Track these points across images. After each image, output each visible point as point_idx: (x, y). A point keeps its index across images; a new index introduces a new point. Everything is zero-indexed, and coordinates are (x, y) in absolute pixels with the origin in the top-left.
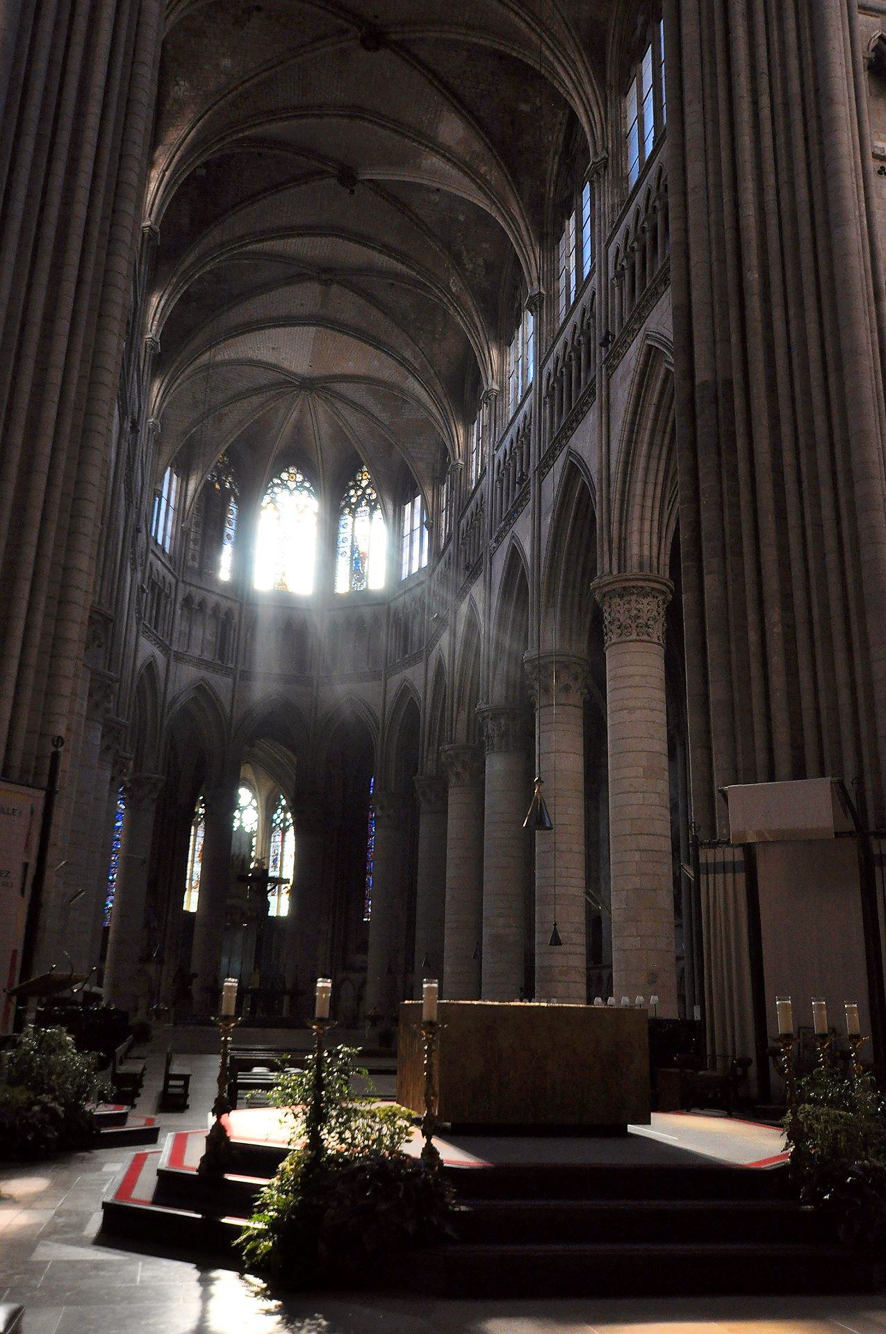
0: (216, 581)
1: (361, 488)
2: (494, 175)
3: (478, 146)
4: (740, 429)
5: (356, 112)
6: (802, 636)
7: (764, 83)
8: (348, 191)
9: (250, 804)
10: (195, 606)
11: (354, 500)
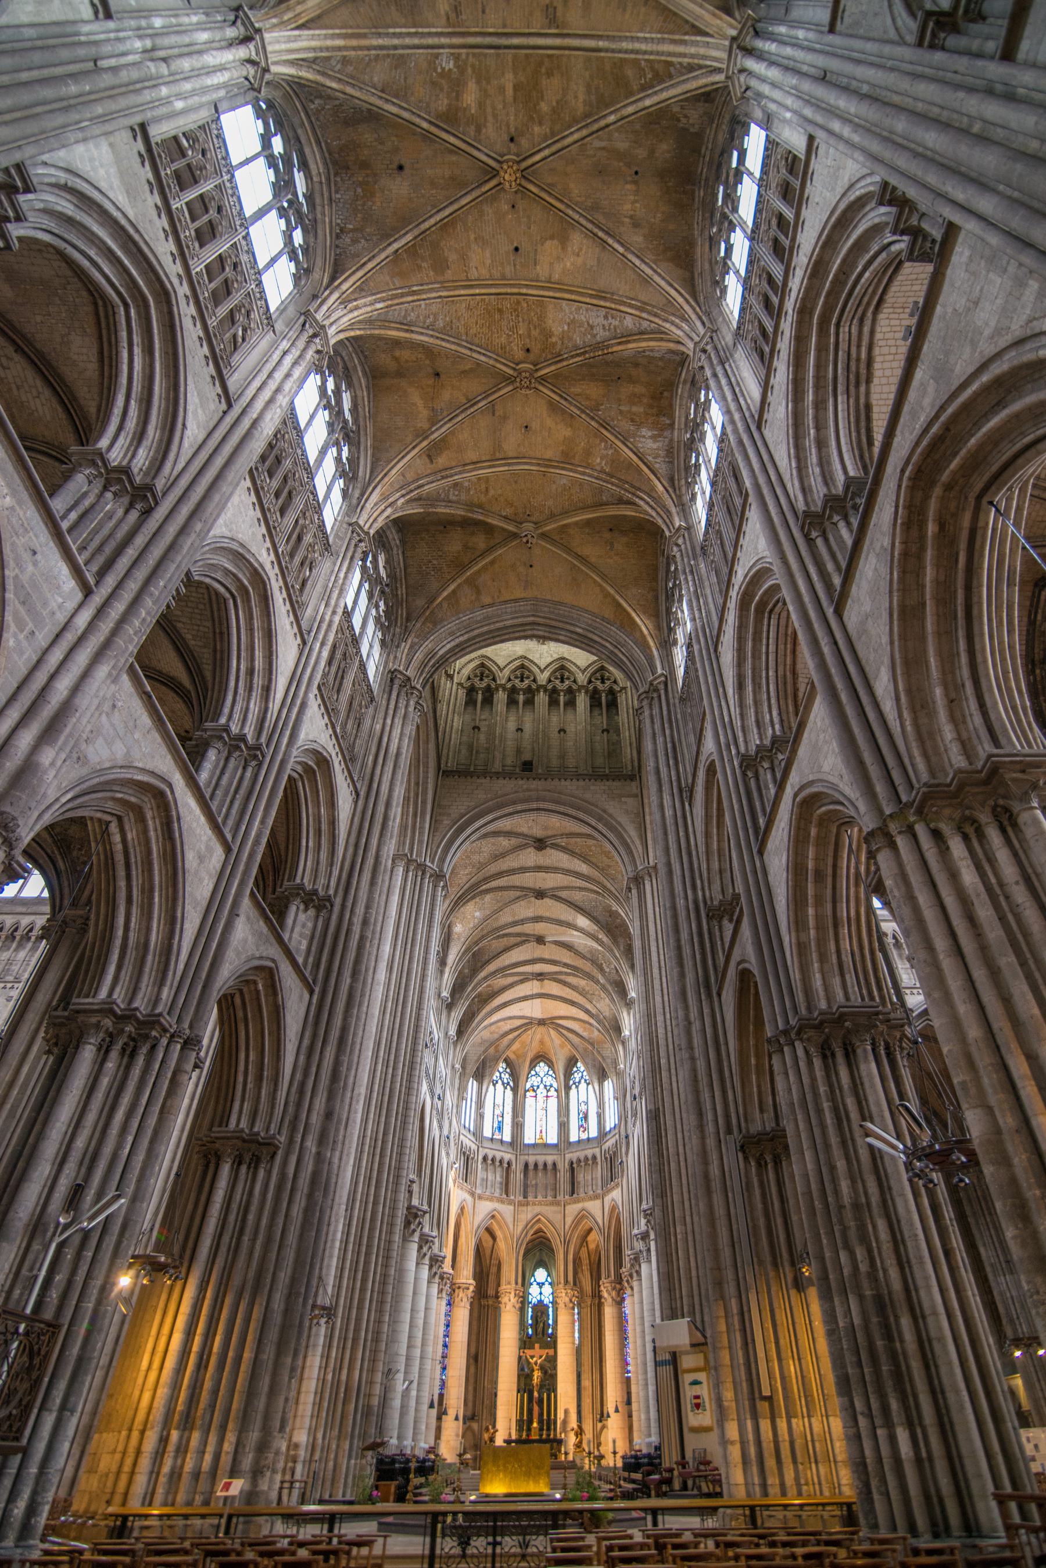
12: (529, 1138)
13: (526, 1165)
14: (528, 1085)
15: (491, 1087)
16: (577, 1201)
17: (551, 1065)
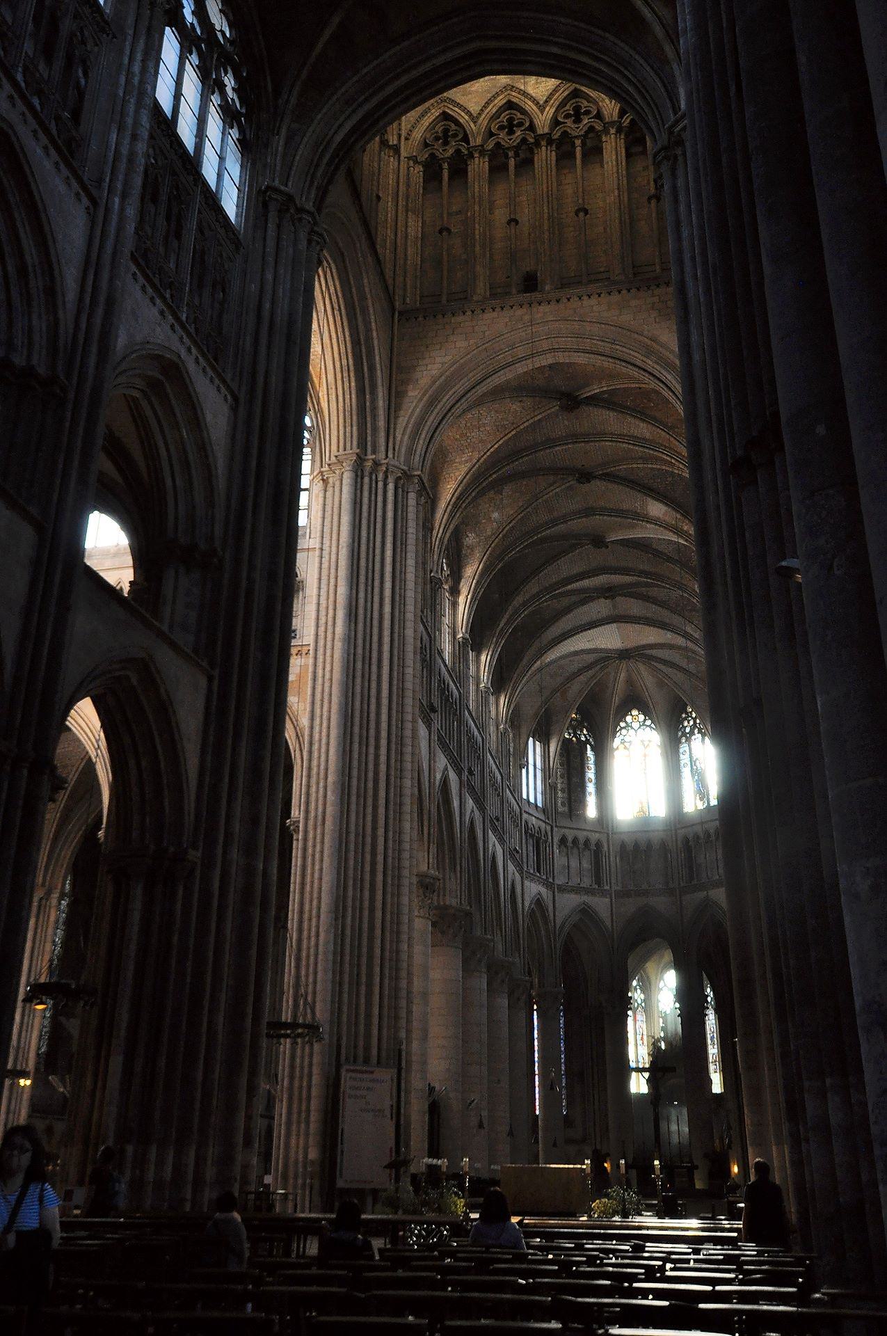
0: (584, 819)
10: (570, 844)
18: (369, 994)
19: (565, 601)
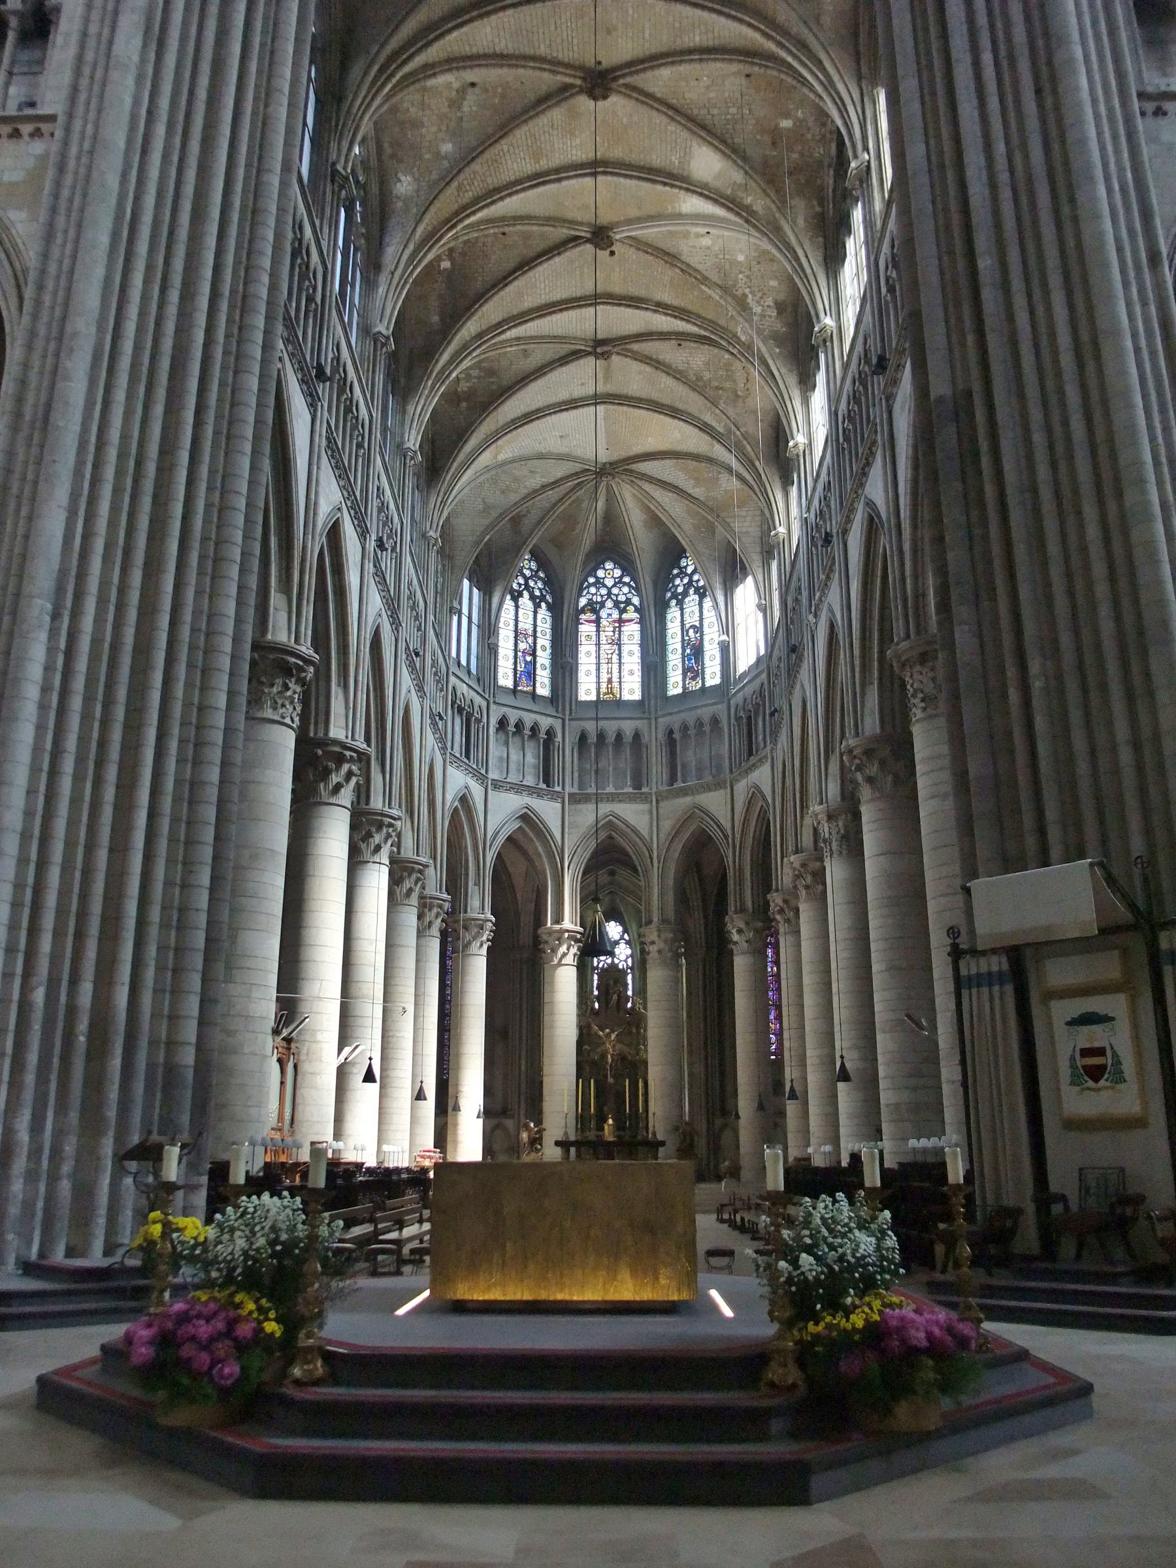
1: (686, 575)
2: (758, 202)
3: (738, 176)
4: (984, 445)
5: (595, 167)
6: (1072, 686)
7: (985, 41)
8: (608, 252)
9: (622, 938)
10: (511, 728)
11: (680, 589)
12: (587, 690)
13: (583, 738)
14: (583, 602)
15: (509, 604)
16: (684, 792)
17: (627, 565)
18: (127, 786)
19: (540, 354)
